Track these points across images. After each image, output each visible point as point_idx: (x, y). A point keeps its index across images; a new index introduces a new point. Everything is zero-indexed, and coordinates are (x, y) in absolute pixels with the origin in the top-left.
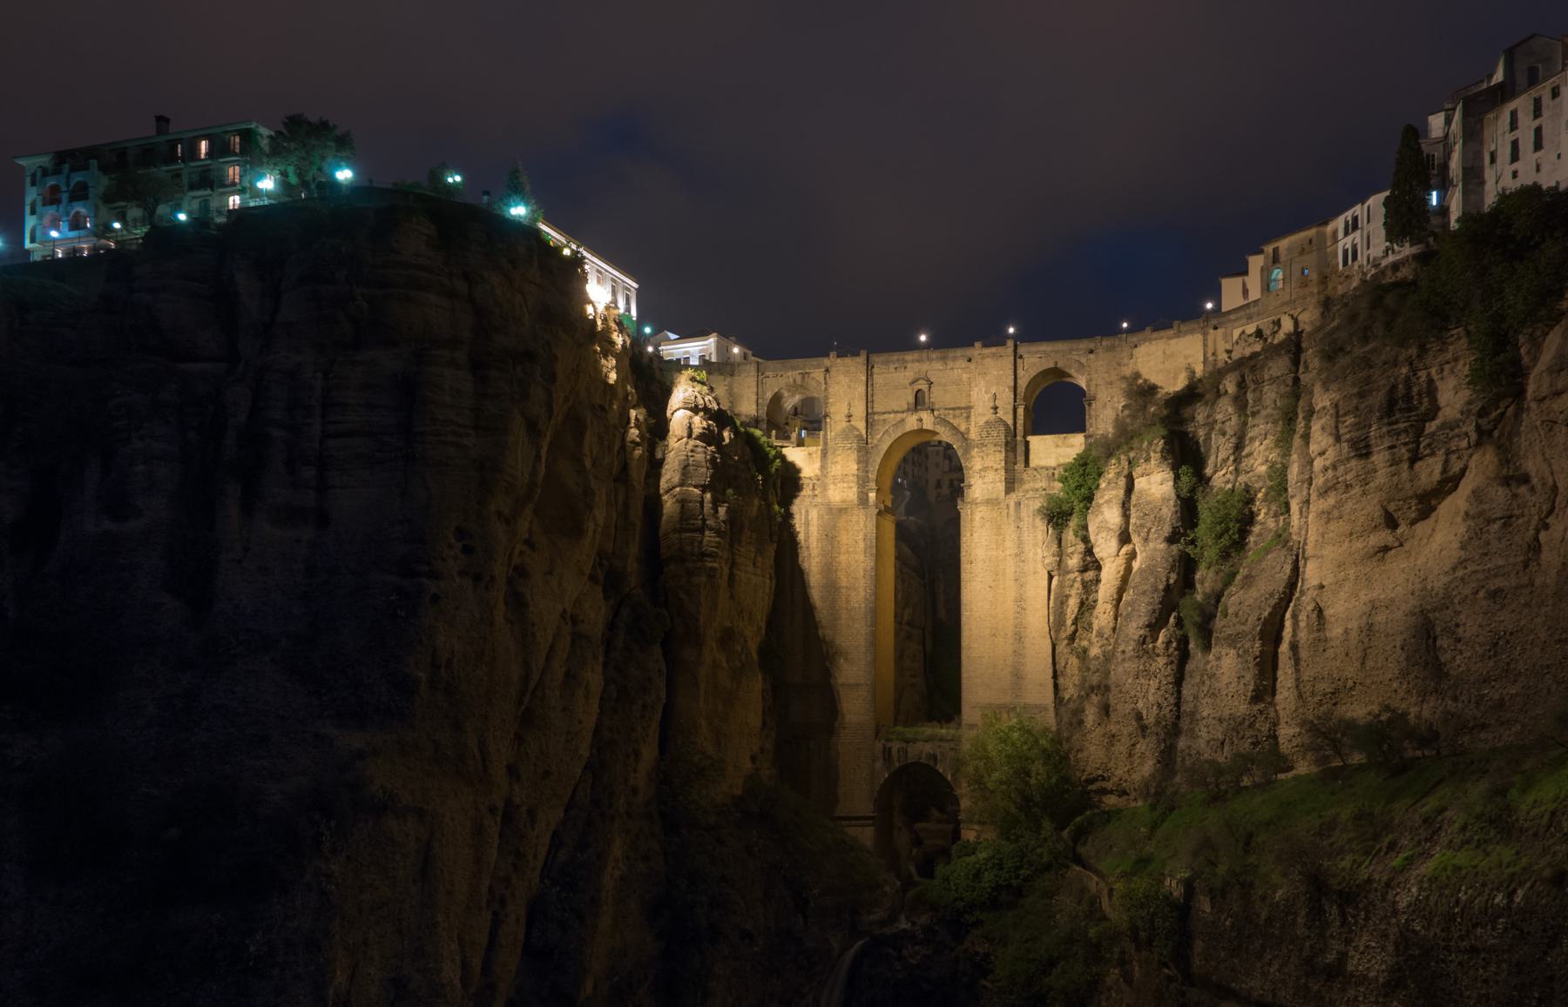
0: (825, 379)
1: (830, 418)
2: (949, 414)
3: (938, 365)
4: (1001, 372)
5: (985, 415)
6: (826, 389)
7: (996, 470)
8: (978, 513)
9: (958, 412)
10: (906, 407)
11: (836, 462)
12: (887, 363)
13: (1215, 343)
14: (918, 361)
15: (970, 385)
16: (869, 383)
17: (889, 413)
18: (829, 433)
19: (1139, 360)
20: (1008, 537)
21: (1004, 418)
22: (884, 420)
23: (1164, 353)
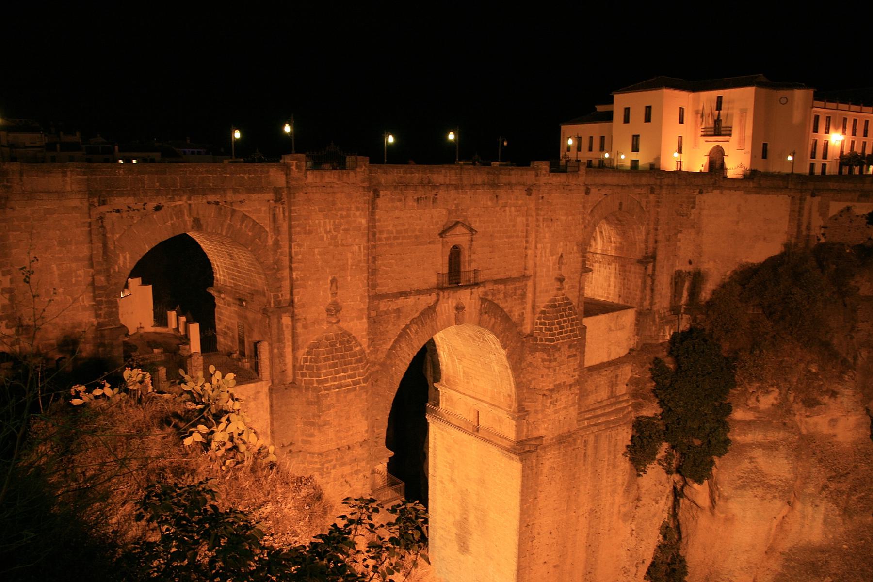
0: (274, 219)
1: (293, 317)
2: (499, 291)
3: (484, 198)
4: (570, 218)
5: (547, 291)
6: (277, 243)
7: (571, 386)
8: (547, 462)
9: (510, 287)
10: (433, 280)
11: (326, 423)
12: (402, 186)
13: (810, 213)
14: (456, 187)
15: (527, 237)
16: (372, 233)
17: (405, 294)
18: (288, 350)
19: (705, 212)
20: (582, 488)
21: (570, 296)
22: (398, 311)
23: (739, 211)
